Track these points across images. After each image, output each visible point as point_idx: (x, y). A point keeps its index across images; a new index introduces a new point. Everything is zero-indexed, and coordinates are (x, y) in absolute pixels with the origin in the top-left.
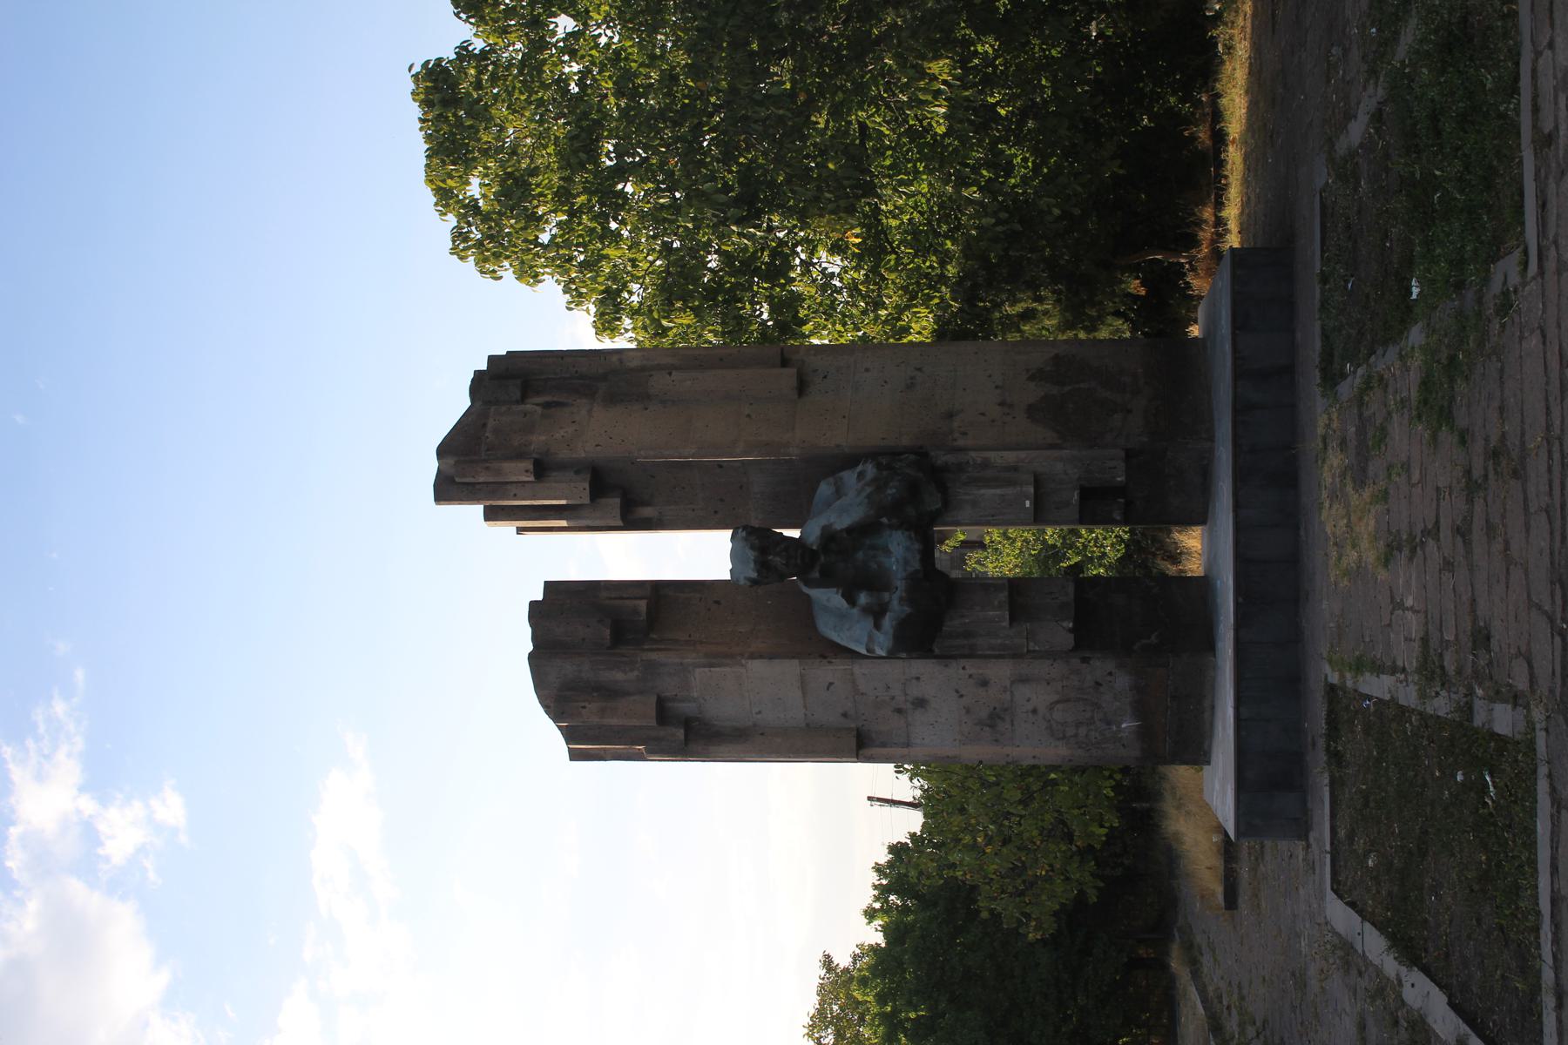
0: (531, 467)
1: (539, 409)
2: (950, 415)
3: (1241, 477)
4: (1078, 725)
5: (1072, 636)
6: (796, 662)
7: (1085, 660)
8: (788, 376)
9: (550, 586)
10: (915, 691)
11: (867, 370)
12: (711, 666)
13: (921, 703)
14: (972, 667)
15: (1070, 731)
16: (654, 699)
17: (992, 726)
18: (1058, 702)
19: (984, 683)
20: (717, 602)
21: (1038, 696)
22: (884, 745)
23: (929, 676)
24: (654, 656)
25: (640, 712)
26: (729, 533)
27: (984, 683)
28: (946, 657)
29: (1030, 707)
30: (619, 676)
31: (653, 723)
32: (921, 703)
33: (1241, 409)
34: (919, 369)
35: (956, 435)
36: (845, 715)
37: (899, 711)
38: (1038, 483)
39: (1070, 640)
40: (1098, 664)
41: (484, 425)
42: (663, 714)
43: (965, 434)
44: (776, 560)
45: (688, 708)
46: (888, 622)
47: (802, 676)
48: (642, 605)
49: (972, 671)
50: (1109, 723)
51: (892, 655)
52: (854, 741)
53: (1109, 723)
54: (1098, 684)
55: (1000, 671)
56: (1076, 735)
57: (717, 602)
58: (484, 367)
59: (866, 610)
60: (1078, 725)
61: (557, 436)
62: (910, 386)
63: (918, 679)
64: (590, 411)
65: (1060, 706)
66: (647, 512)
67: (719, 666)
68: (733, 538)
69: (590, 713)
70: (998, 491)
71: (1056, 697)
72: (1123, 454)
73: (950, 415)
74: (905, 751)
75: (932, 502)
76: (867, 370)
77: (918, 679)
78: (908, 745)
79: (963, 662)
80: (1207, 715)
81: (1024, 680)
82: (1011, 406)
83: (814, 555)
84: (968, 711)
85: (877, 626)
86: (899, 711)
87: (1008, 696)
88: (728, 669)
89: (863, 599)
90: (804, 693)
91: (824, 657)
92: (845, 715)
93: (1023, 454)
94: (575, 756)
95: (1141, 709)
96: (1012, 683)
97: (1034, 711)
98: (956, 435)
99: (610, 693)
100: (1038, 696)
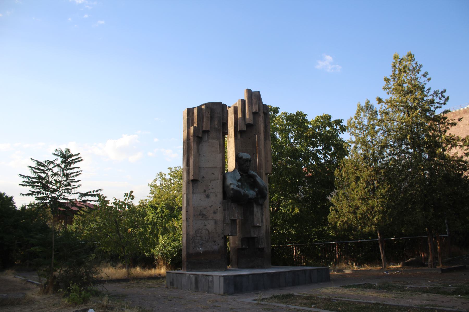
3: (294, 272)
4: (201, 237)
6: (221, 166)
10: (211, 195)
12: (220, 145)
13: (208, 196)
15: (198, 235)
17: (200, 215)
18: (208, 231)
21: (210, 226)
22: (193, 187)
23: (217, 198)
25: (206, 126)
28: (223, 204)
29: (207, 224)
31: (204, 129)
32: (208, 196)
37: (205, 191)
38: (259, 227)
42: (206, 132)
45: (205, 138)
47: (216, 167)
49: (219, 209)
50: (201, 245)
53: (201, 245)
54: (215, 242)
55: (219, 217)
56: (197, 236)
60: (201, 237)
65: (207, 232)
66: (239, 136)
67: (220, 147)
69: (208, 114)
71: (210, 230)
74: (191, 191)
78: (193, 193)
80: (205, 270)
81: (216, 222)
84: (205, 208)
86: (205, 191)
87: (210, 218)
88: (218, 149)
92: (203, 177)
95: (205, 253)
97: (205, 225)
99: (212, 118)
100: (210, 226)
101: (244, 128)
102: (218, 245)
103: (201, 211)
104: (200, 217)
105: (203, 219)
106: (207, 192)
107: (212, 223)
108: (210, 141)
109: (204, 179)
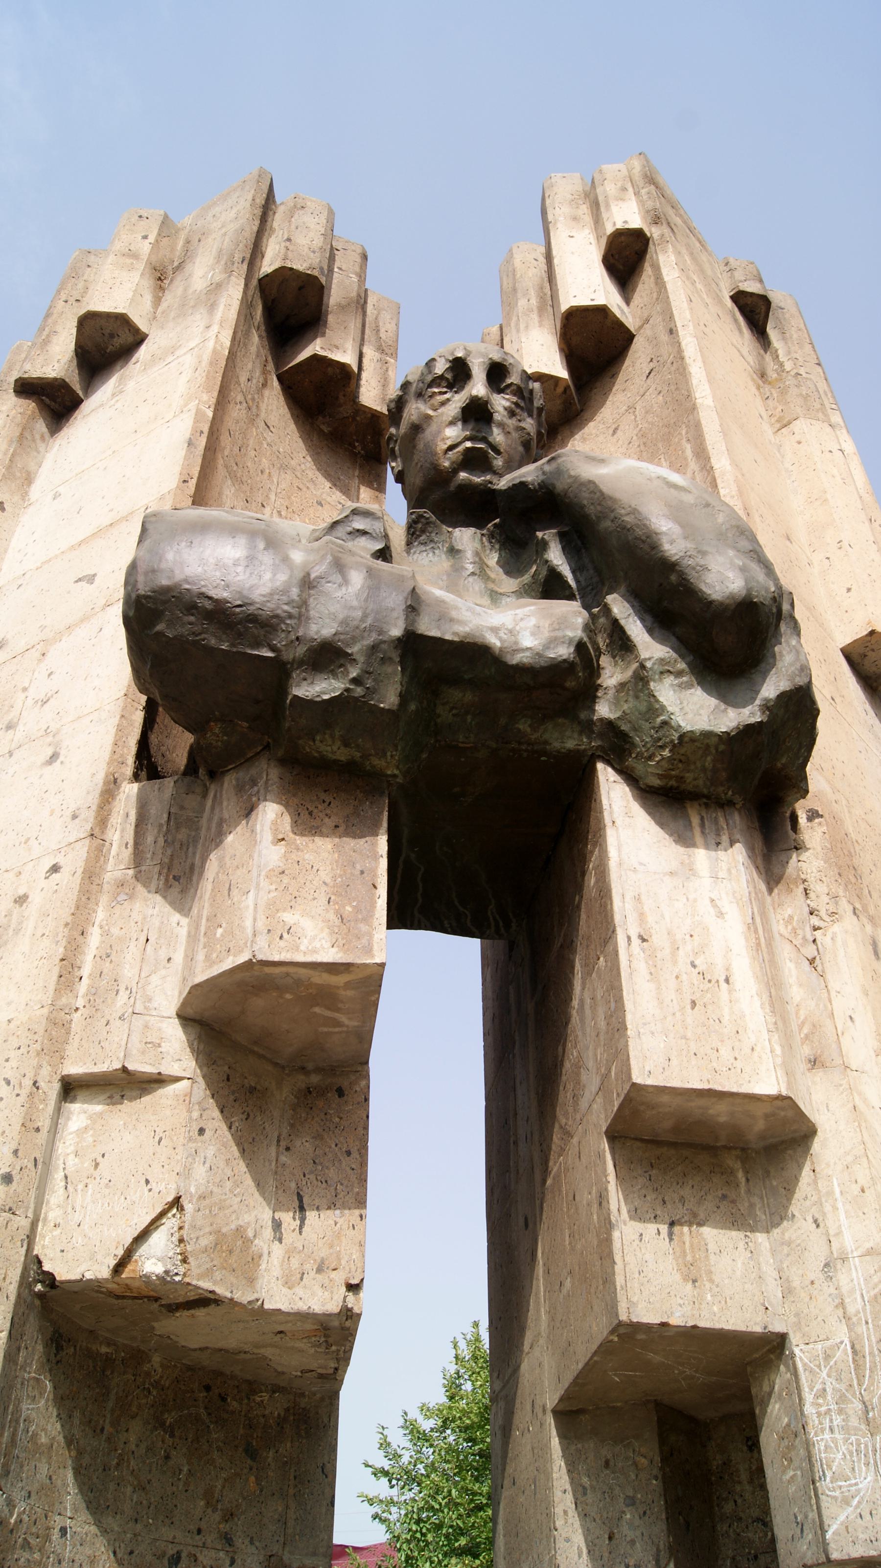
48: (346, 357)
79: (75, 861)
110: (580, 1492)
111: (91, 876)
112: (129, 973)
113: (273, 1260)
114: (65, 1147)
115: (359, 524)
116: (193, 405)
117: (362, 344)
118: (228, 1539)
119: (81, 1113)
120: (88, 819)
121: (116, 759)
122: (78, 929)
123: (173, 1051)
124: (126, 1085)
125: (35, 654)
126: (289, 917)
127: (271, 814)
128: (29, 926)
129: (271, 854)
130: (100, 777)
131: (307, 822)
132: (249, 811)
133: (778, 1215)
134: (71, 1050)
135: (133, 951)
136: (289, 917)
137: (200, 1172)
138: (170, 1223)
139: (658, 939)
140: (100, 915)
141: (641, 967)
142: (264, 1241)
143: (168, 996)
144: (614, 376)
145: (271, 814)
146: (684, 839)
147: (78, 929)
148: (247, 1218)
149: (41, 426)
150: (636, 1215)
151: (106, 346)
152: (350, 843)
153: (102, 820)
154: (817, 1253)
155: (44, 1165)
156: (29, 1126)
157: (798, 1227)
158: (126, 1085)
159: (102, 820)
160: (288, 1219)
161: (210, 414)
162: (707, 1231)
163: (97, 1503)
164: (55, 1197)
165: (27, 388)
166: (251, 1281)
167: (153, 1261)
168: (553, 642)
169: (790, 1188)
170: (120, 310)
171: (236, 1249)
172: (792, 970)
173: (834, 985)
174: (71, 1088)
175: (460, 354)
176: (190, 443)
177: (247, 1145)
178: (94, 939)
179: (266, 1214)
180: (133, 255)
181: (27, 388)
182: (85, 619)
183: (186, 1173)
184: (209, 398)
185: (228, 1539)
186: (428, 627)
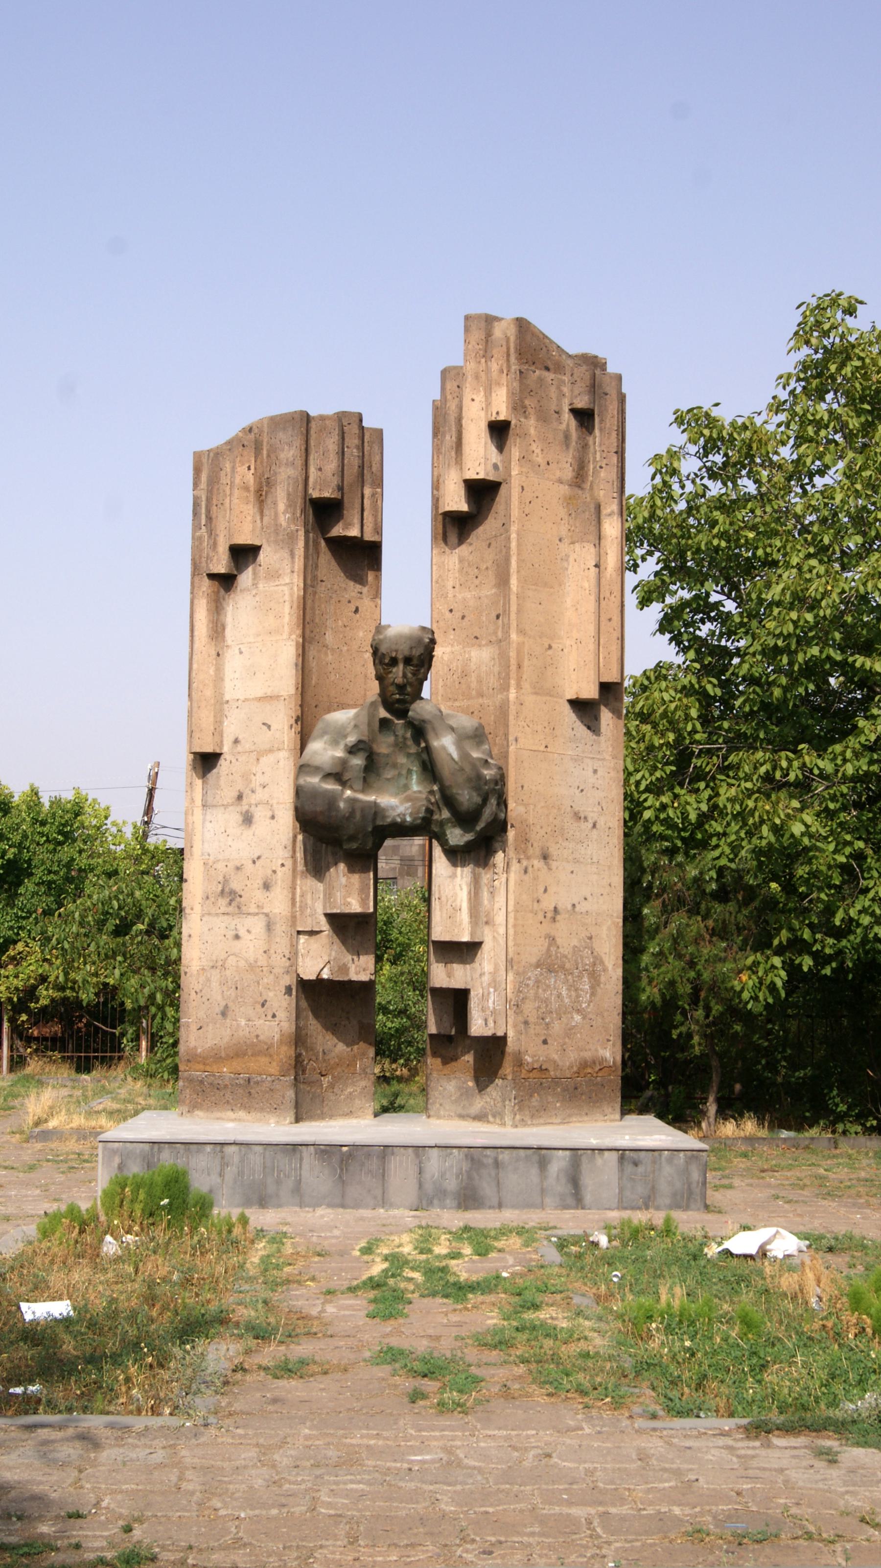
0: (502, 417)
1: (563, 426)
2: (545, 857)
5: (313, 977)
7: (288, 990)
8: (590, 692)
9: (379, 434)
10: (260, 814)
11: (595, 771)
13: (248, 819)
14: (283, 875)
16: (258, 543)
19: (267, 886)
20: (357, 611)
24: (301, 544)
26: (428, 625)
27: (267, 886)
29: (242, 932)
30: (281, 506)
32: (248, 819)
33: (540, 1154)
34: (594, 826)
35: (525, 863)
36: (236, 741)
37: (240, 797)
39: (309, 974)
40: (285, 1004)
41: (547, 369)
42: (244, 554)
43: (526, 872)
44: (398, 673)
46: (331, 786)
47: (277, 697)
51: (299, 792)
52: (208, 749)
55: (278, 903)
57: (357, 611)
58: (611, 369)
59: (344, 763)
61: (534, 447)
62: (577, 817)
63: (273, 817)
64: (560, 481)
68: (424, 629)
69: (244, 474)
70: (465, 906)
72: (500, 1033)
73: (545, 857)
75: (457, 836)
76: (595, 771)
77: (273, 817)
79: (289, 864)
80: (230, 1114)
81: (269, 927)
82: (554, 919)
83: (402, 713)
84: (238, 868)
85: (328, 776)
86: (240, 797)
87: (253, 909)
88: (287, 619)
89: (358, 761)
90: (260, 699)
91: (296, 722)
93: (502, 930)
94: (198, 458)
96: (267, 915)
97: (237, 937)
98: (525, 863)
101: (463, 506)
102: (274, 1016)
103: (226, 881)
104: (223, 902)
105: (230, 909)
106: (245, 801)
107: (257, 925)
108: (261, 586)
109: (239, 748)
110: (434, 1010)
111: (294, 870)
112: (309, 902)
113: (353, 969)
114: (300, 947)
115: (361, 746)
116: (294, 637)
117: (363, 487)
118: (348, 1018)
119: (303, 939)
120: (290, 848)
121: (294, 828)
122: (293, 888)
123: (323, 924)
124: (312, 933)
125: (254, 756)
126: (349, 900)
127: (342, 866)
128: (279, 882)
129: (343, 880)
130: (291, 835)
131: (351, 870)
132: (336, 864)
133: (472, 961)
134: (298, 923)
135: (309, 896)
136: (349, 900)
137: (333, 953)
138: (328, 966)
139: (443, 899)
140: (299, 882)
141: (438, 907)
142: (350, 965)
143: (320, 909)
144: (493, 500)
145: (342, 866)
146: (454, 864)
147: (293, 888)
148: (345, 960)
149: (222, 592)
150: (437, 962)
151: (244, 554)
152: (363, 875)
153: (294, 851)
154: (479, 972)
155: (296, 953)
156: (292, 946)
157: (476, 965)
158: (312, 933)
159: (294, 851)
160: (355, 958)
161: (301, 640)
162: (455, 965)
163: (316, 1016)
164: (300, 960)
165: (212, 576)
166: (348, 974)
167: (325, 975)
168: (415, 819)
169: (476, 955)
170: (249, 542)
171: (344, 969)
172: (485, 894)
173: (496, 899)
174: (299, 933)
175: (394, 655)
176: (296, 665)
177: (344, 942)
178: (298, 890)
179: (350, 957)
180: (246, 488)
181: (212, 576)
182: (271, 751)
183: (330, 955)
184: (299, 632)
185: (348, 1018)
186: (379, 822)
